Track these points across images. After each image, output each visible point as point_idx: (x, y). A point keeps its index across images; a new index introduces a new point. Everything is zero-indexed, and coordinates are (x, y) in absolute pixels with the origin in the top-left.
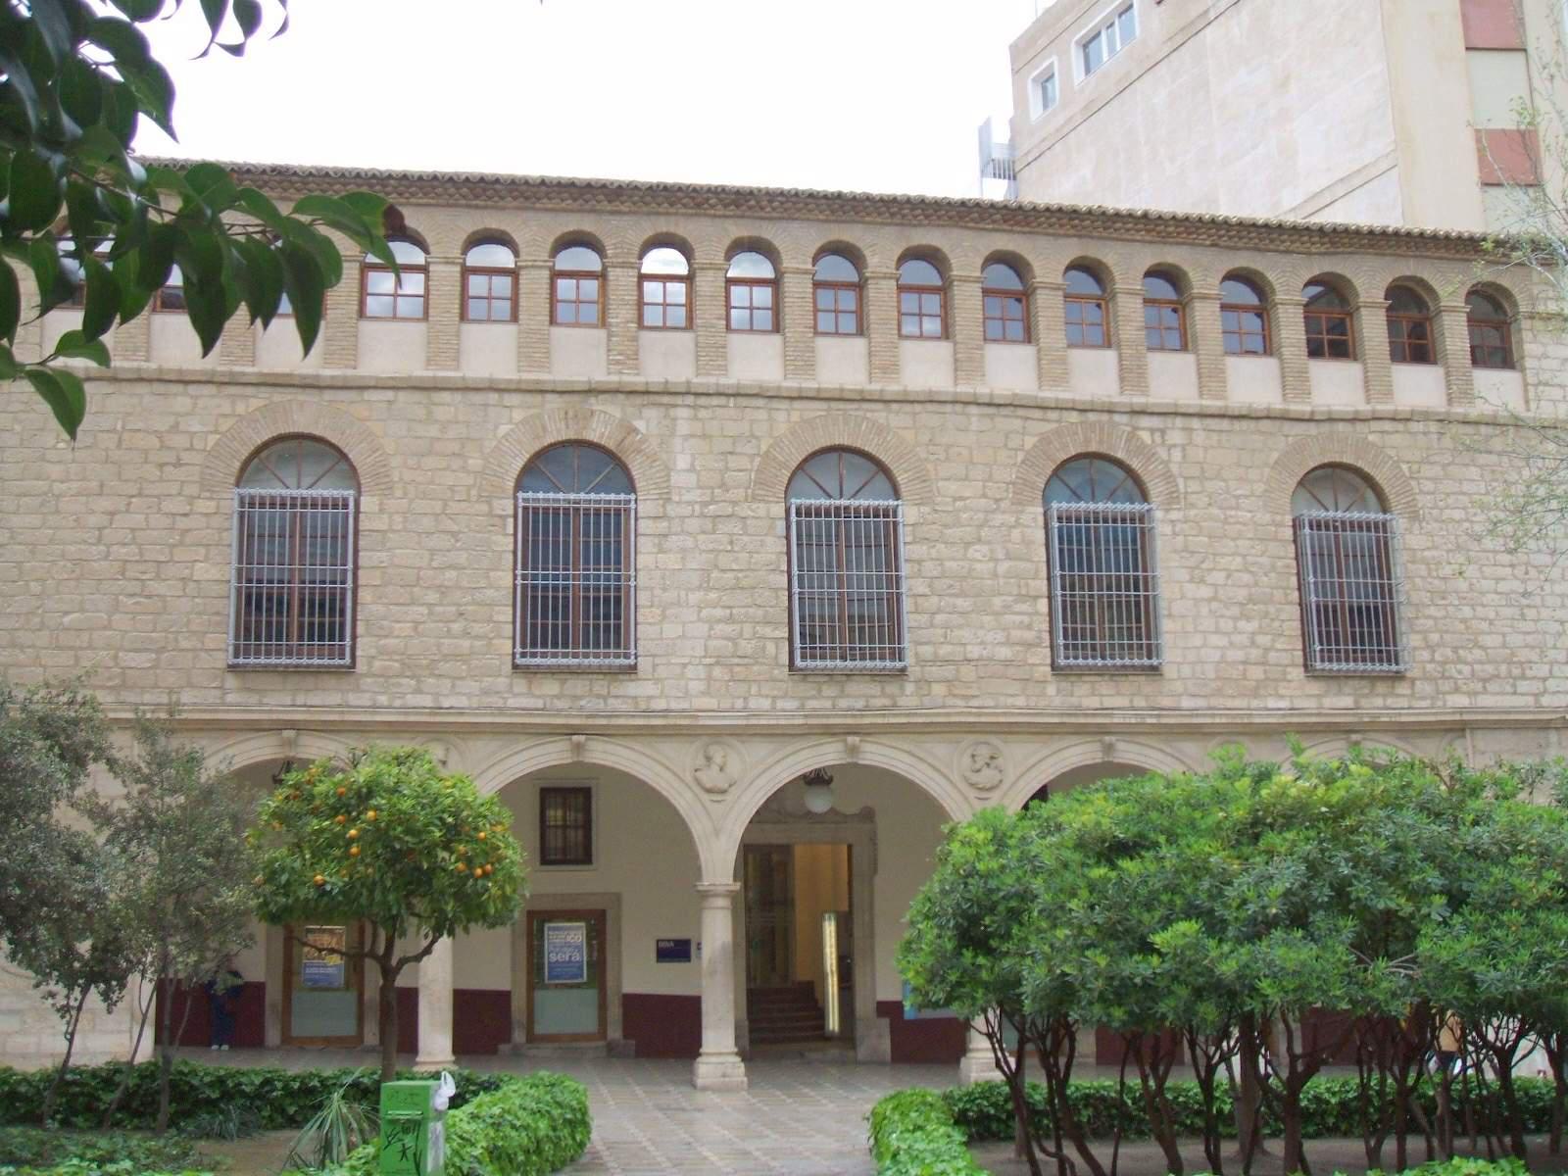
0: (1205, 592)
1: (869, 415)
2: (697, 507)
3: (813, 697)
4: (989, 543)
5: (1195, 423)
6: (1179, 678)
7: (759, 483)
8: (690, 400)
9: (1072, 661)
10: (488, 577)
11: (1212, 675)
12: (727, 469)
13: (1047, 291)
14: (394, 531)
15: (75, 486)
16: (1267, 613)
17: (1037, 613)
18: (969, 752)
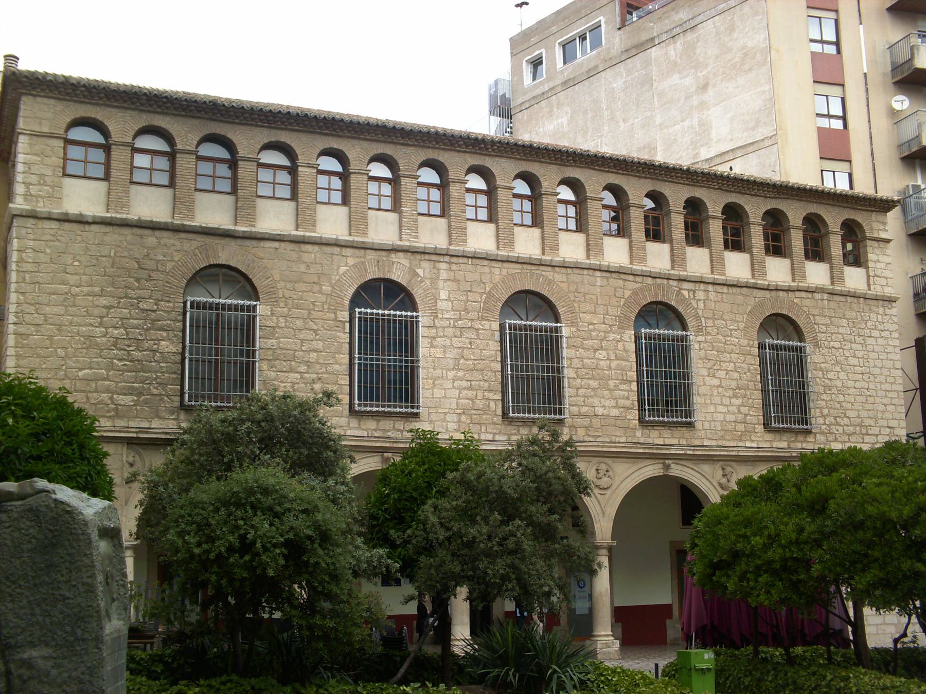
0: (716, 382)
1: (543, 273)
2: (452, 322)
3: (515, 434)
4: (606, 350)
5: (710, 288)
6: (703, 429)
7: (486, 309)
8: (447, 259)
9: (652, 418)
10: (335, 357)
11: (719, 428)
12: (468, 301)
13: (635, 208)
14: (279, 327)
15: (86, 289)
16: (746, 395)
17: (631, 390)
18: (594, 468)
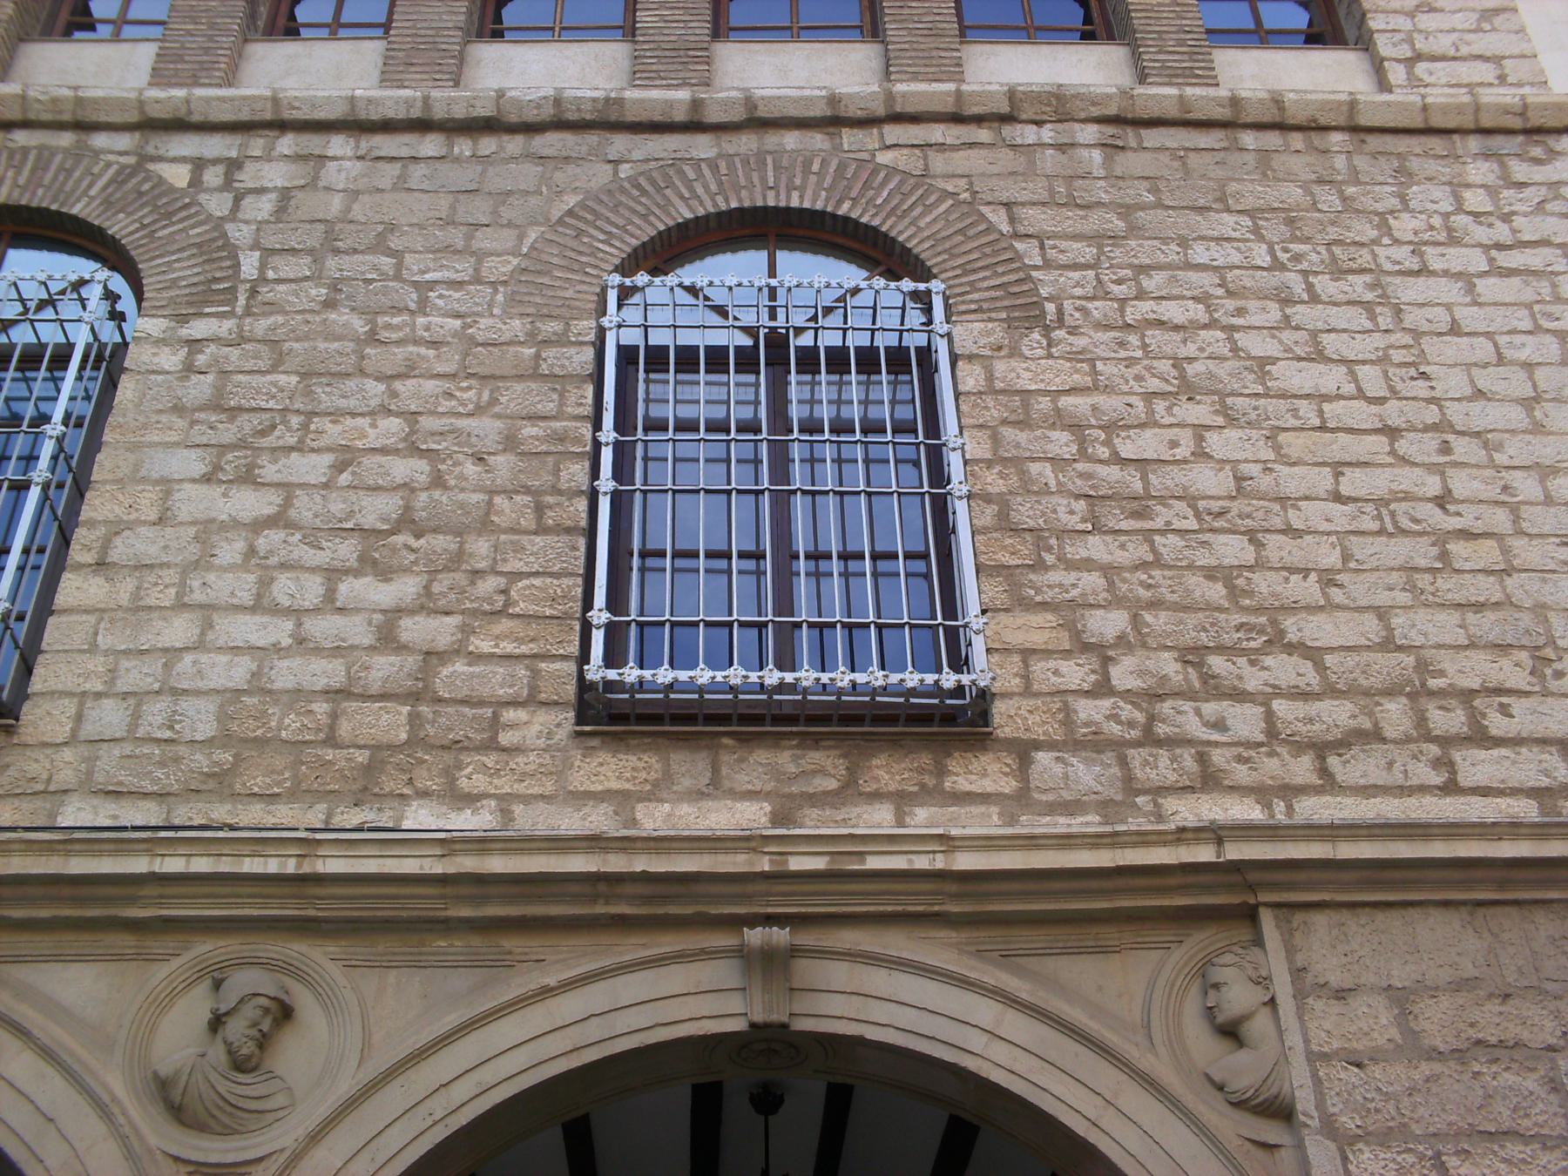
5: (338, 145)
11: (206, 728)
